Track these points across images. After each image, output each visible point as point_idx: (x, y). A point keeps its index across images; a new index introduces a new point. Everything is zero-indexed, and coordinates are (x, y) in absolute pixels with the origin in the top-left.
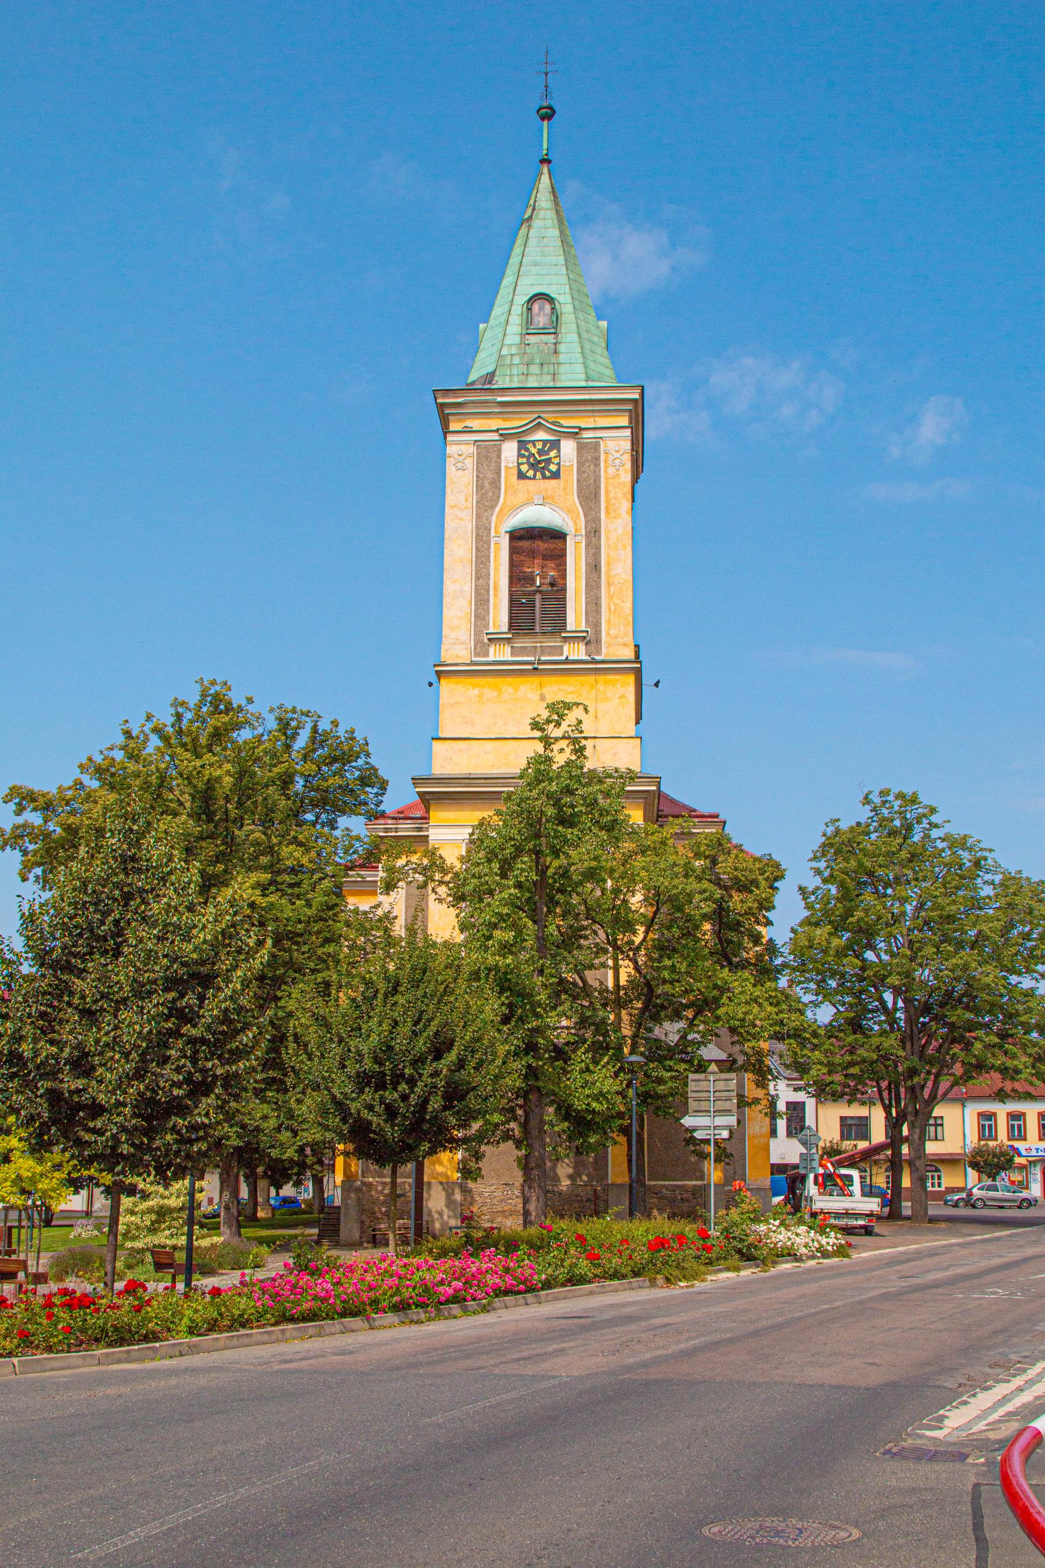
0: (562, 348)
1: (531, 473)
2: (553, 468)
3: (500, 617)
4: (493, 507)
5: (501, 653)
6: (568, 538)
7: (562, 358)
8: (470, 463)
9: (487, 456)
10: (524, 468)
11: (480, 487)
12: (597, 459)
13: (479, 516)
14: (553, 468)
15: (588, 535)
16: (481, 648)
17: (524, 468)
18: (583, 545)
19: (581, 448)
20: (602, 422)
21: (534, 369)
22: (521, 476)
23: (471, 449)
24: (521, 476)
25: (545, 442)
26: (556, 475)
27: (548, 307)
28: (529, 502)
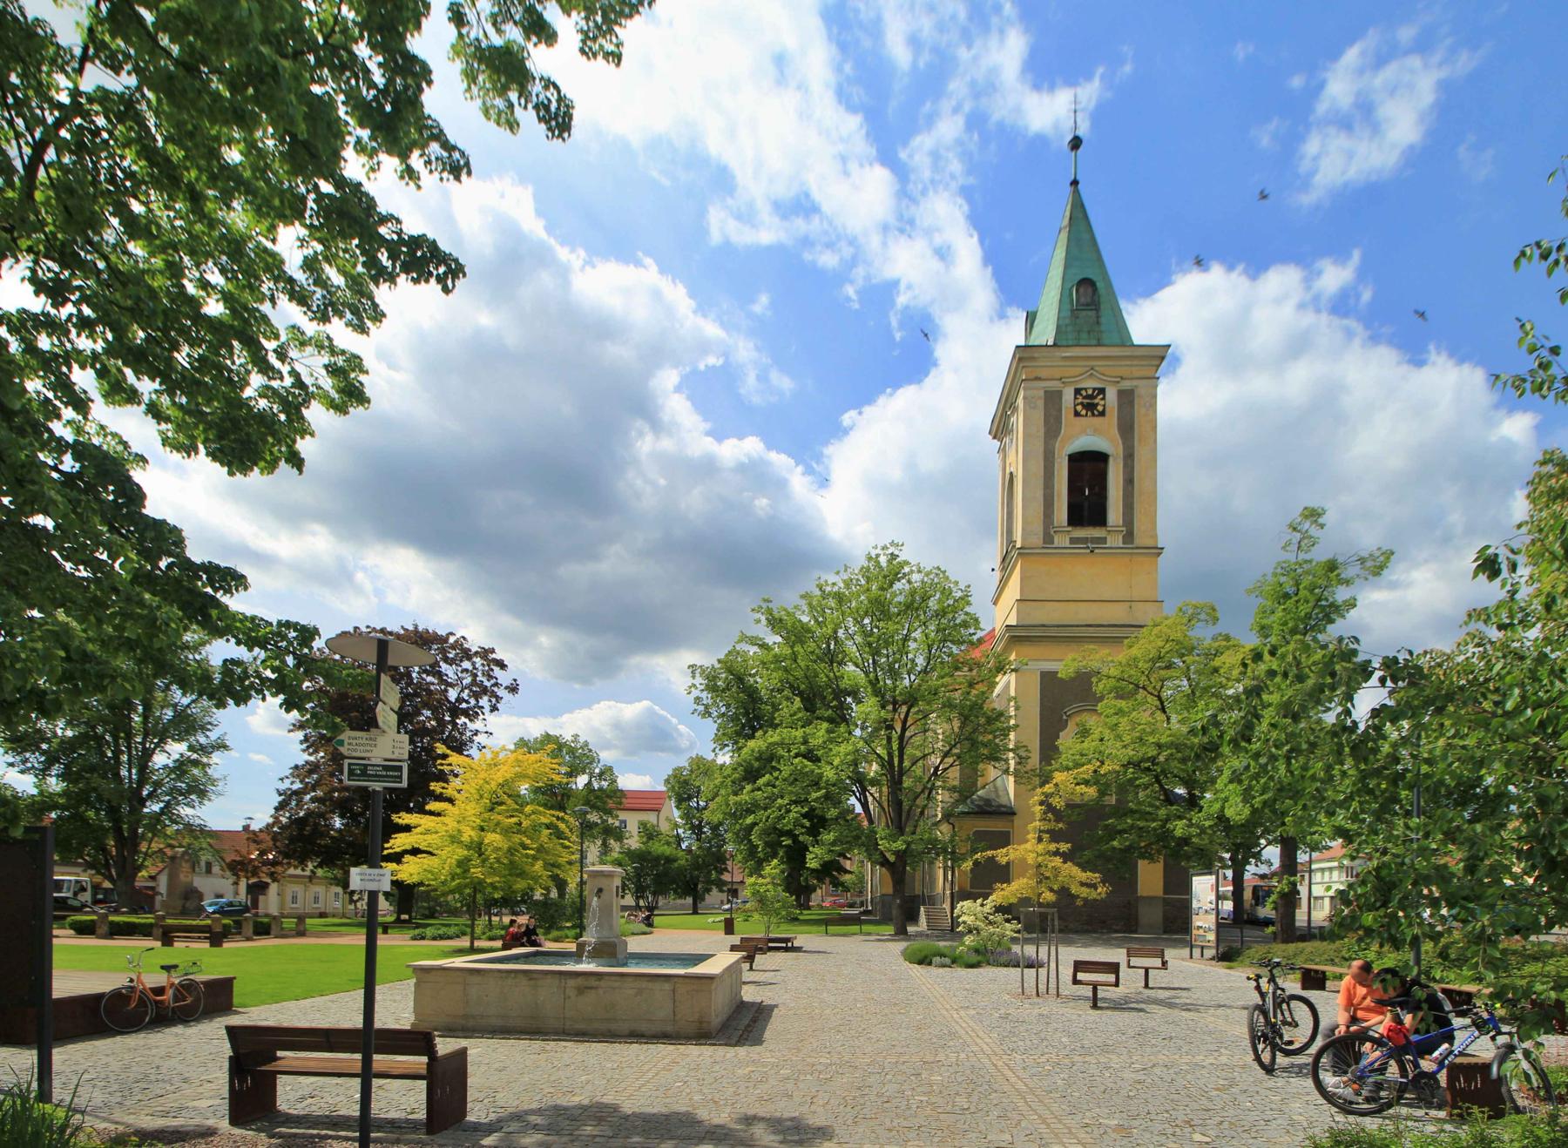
0: (1103, 320)
2: (1100, 408)
4: (1056, 437)
6: (1111, 461)
7: (1103, 328)
8: (1041, 403)
9: (1053, 398)
10: (1079, 408)
13: (1046, 443)
14: (1100, 408)
15: (1125, 458)
16: (1048, 539)
17: (1079, 408)
19: (1121, 393)
20: (1137, 372)
21: (1084, 336)
22: (1077, 414)
23: (1042, 393)
24: (1077, 414)
26: (1102, 414)
27: (1090, 290)
28: (1084, 432)
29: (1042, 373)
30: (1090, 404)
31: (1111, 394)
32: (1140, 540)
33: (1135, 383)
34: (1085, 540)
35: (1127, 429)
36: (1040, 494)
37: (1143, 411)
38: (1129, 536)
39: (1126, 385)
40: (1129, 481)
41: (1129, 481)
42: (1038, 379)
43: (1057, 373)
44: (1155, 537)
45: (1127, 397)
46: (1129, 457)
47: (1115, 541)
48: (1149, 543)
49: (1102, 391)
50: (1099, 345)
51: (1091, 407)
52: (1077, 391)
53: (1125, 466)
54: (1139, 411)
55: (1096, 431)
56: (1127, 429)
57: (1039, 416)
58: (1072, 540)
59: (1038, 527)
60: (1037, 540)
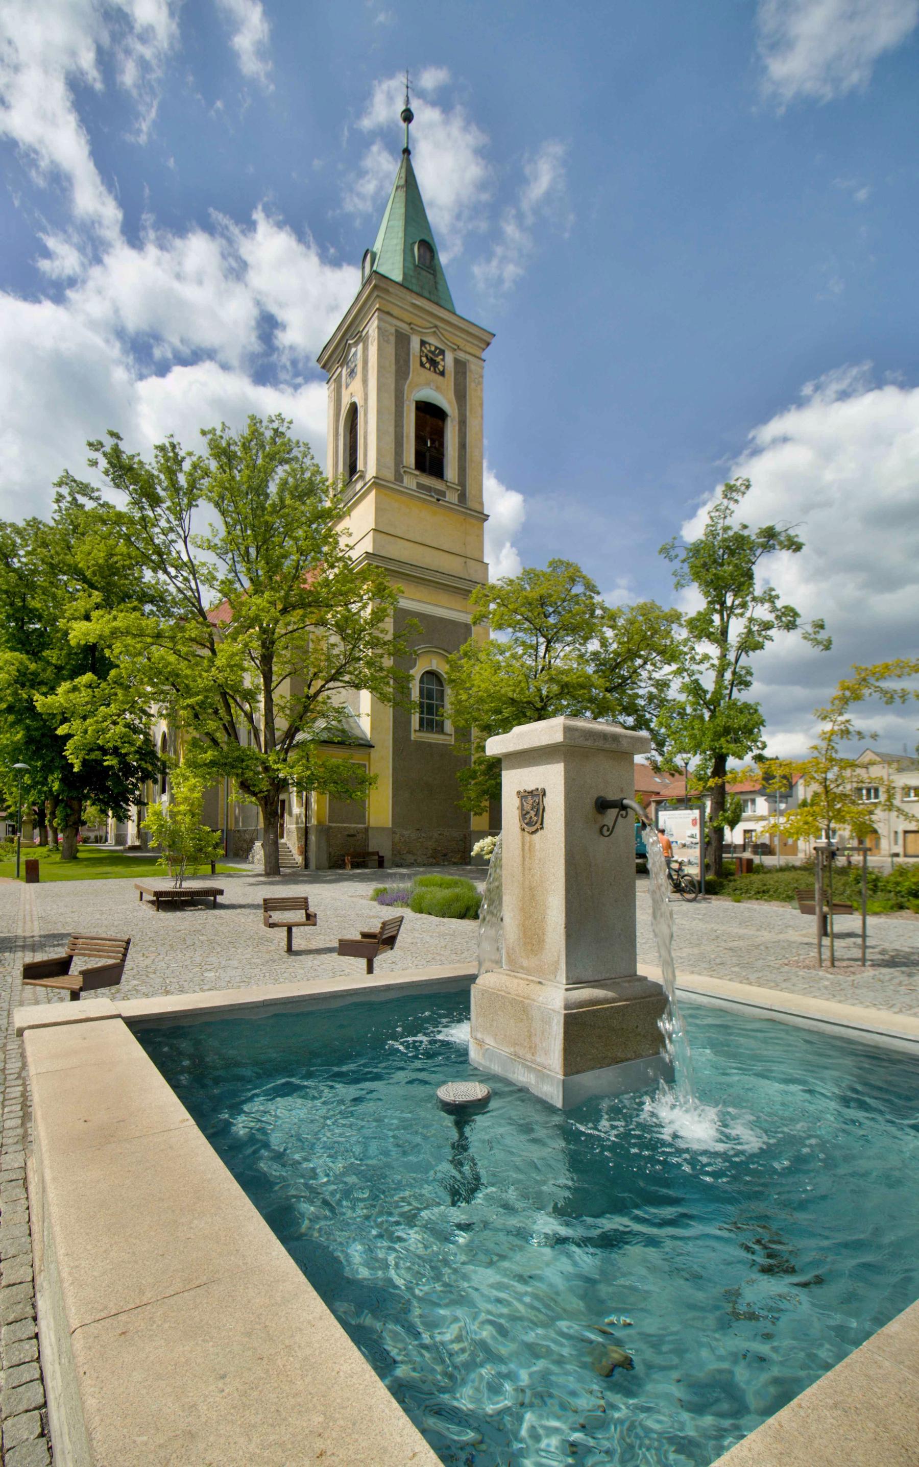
1: (427, 365)
3: (410, 458)
4: (406, 379)
5: (410, 482)
8: (392, 339)
10: (424, 359)
11: (397, 361)
12: (465, 373)
14: (441, 368)
16: (399, 478)
18: (457, 428)
19: (457, 361)
23: (393, 330)
24: (422, 365)
25: (436, 348)
26: (442, 374)
28: (428, 384)
29: (396, 312)
30: (432, 362)
31: (449, 358)
32: (471, 504)
33: (468, 357)
34: (429, 489)
35: (461, 395)
36: (392, 429)
37: (473, 385)
38: (463, 497)
39: (462, 356)
40: (463, 446)
41: (463, 446)
42: (391, 315)
43: (407, 317)
44: (482, 504)
45: (460, 365)
46: (463, 423)
47: (452, 497)
48: (478, 508)
49: (442, 352)
50: (437, 304)
51: (434, 363)
52: (423, 343)
53: (460, 430)
54: (471, 386)
55: (438, 389)
56: (461, 395)
57: (391, 349)
58: (419, 486)
59: (390, 461)
60: (390, 475)
